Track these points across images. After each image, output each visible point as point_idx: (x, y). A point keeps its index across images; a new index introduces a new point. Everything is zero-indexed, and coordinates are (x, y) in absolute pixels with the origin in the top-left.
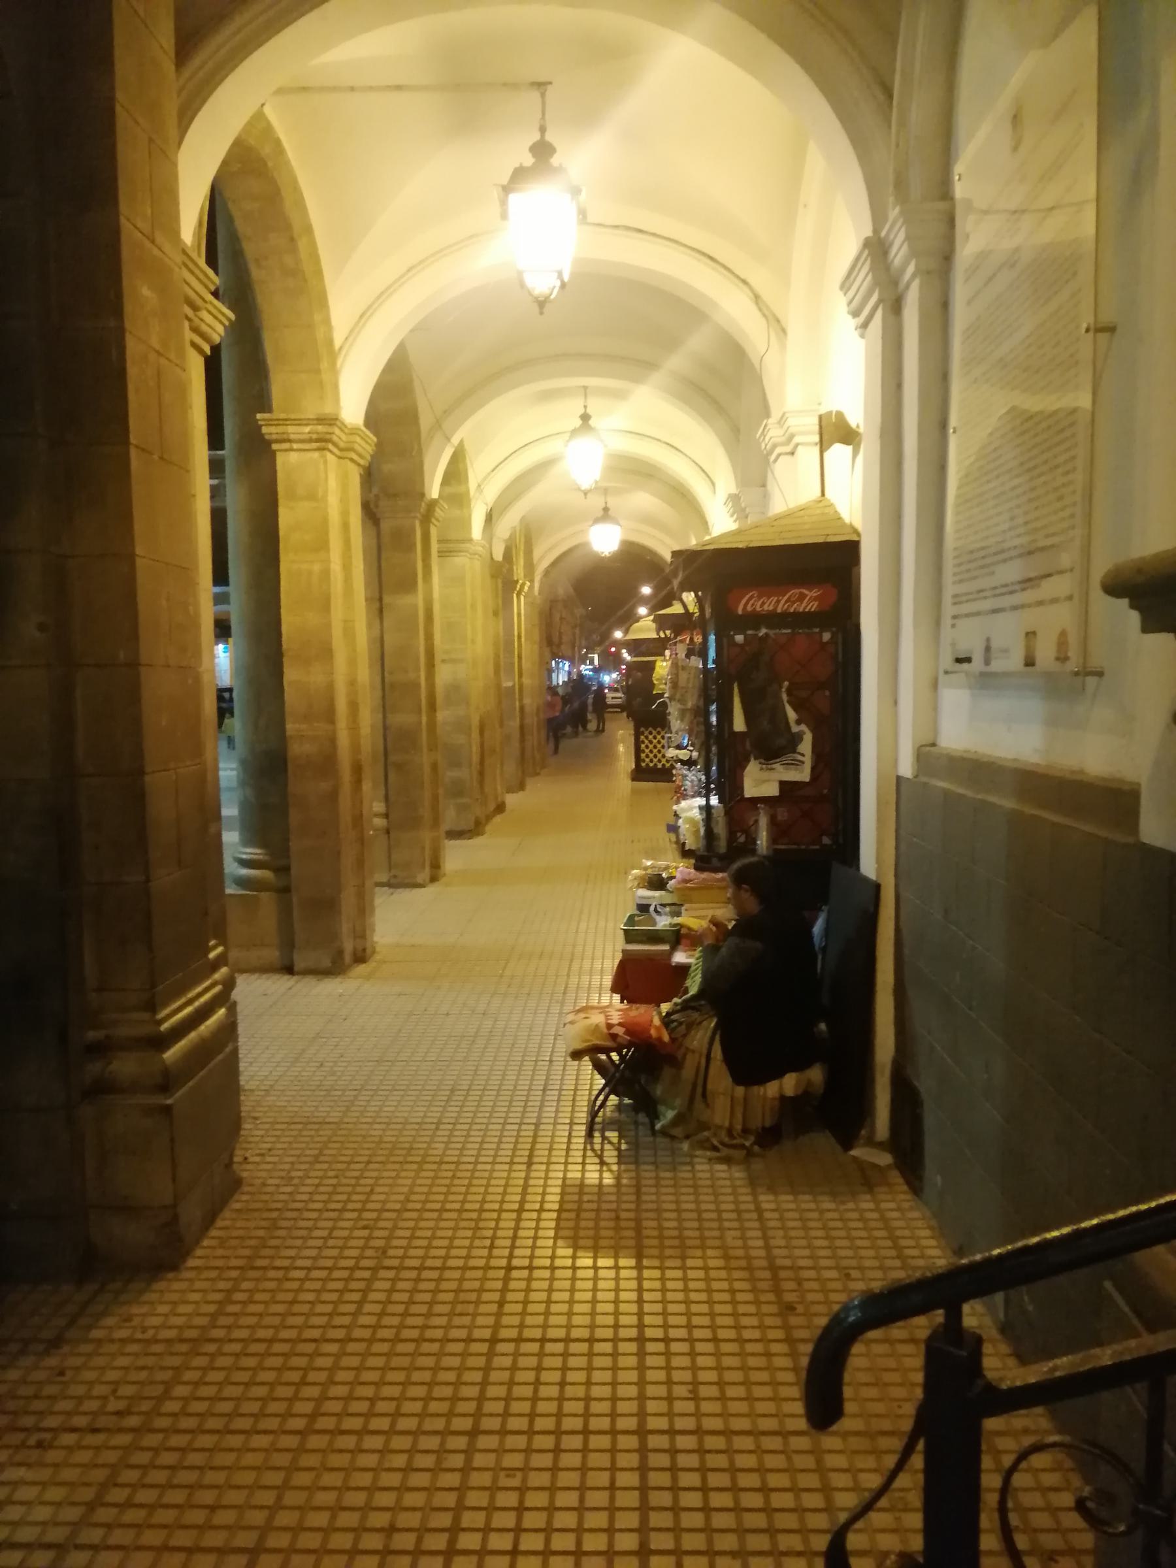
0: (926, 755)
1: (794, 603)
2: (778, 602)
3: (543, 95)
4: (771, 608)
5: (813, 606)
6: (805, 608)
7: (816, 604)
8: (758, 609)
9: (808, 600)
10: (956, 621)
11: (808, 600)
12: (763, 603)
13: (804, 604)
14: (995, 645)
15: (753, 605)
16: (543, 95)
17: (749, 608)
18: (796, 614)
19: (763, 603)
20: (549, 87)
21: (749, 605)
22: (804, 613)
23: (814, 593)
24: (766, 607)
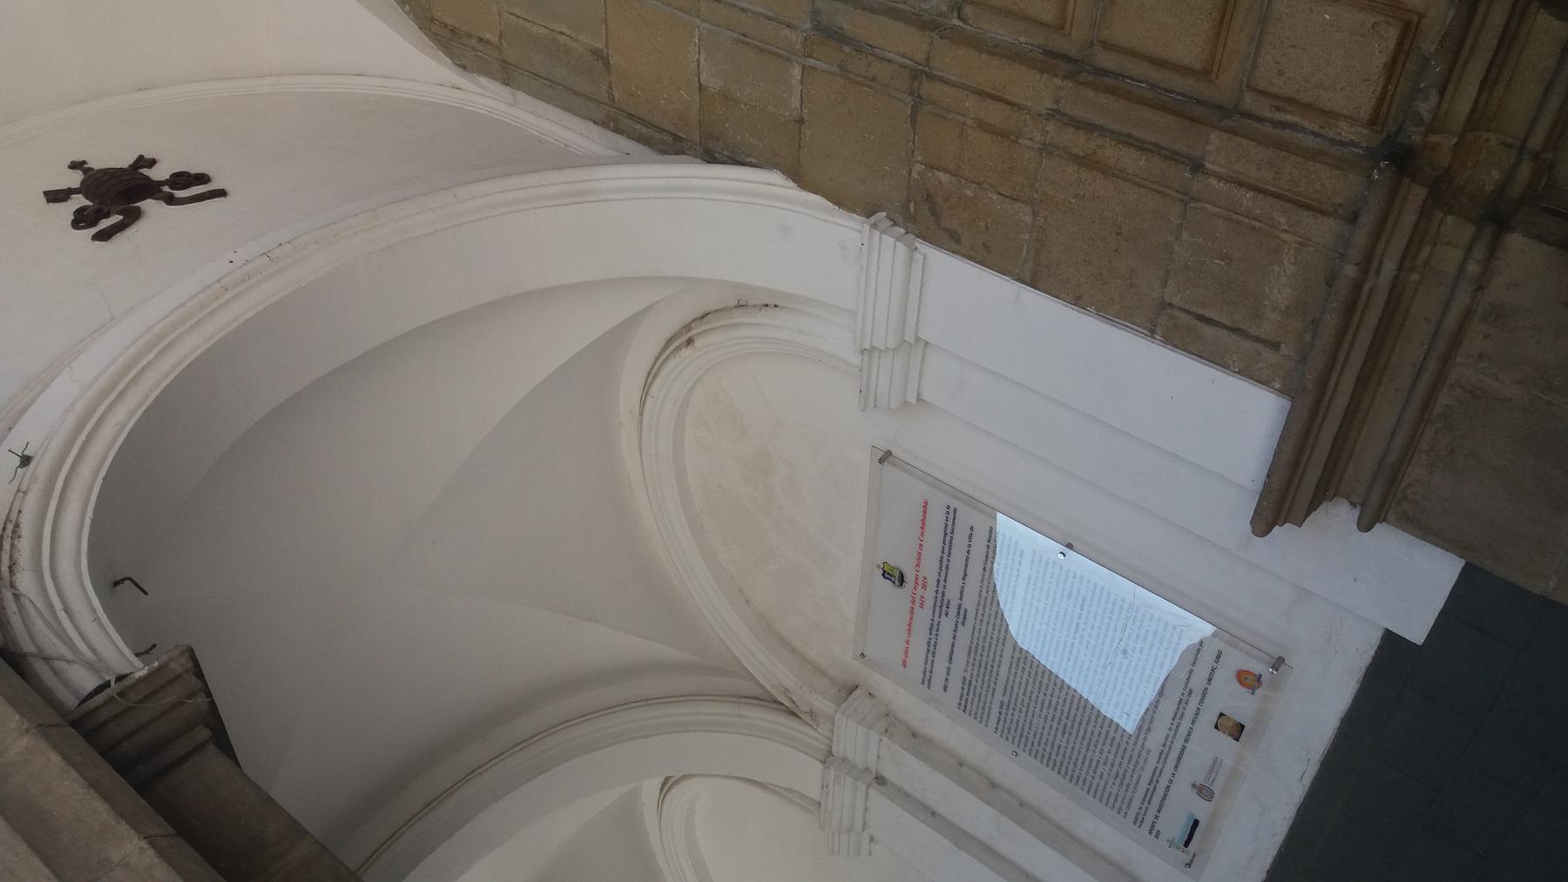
10: (1154, 832)
14: (1200, 781)
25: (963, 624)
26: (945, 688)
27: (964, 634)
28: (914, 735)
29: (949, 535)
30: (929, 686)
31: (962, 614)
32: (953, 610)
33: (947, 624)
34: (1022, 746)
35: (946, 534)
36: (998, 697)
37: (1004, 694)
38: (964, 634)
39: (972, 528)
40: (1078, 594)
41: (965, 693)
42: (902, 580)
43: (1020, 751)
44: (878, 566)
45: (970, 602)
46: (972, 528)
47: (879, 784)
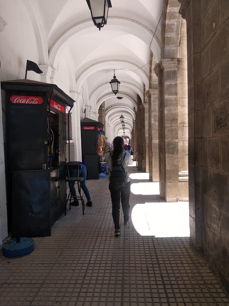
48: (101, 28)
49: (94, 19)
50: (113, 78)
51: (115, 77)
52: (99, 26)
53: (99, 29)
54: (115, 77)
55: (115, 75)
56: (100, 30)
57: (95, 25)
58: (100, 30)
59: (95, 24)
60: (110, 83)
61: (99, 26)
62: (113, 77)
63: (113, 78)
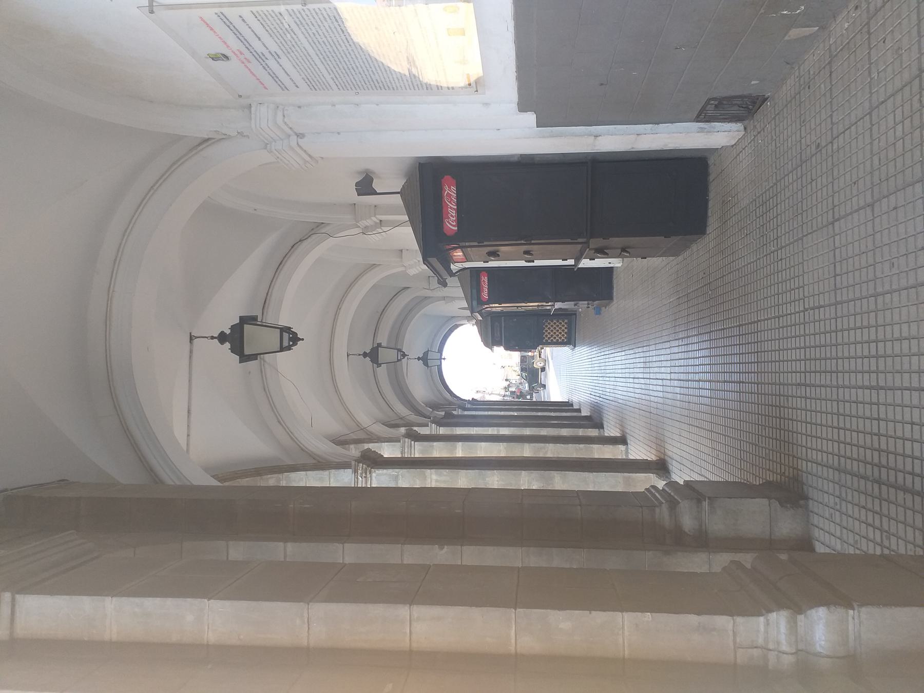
0: (523, 107)
1: (452, 200)
2: (451, 208)
3: (197, 337)
4: (454, 212)
5: (453, 188)
6: (454, 193)
7: (452, 187)
8: (454, 219)
9: (450, 192)
11: (450, 192)
12: (452, 216)
13: (453, 194)
15: (452, 221)
16: (197, 337)
17: (454, 224)
18: (457, 198)
19: (452, 216)
20: (192, 334)
21: (452, 223)
22: (457, 194)
23: (446, 188)
24: (454, 215)
25: (279, 57)
26: (297, 86)
27: (284, 61)
28: (299, 107)
29: (231, 26)
30: (288, 90)
31: (276, 56)
32: (268, 55)
33: (272, 63)
34: (358, 89)
35: (228, 26)
36: (328, 77)
37: (330, 74)
38: (284, 61)
39: (240, 16)
40: (329, 16)
41: (309, 83)
42: (227, 58)
43: (359, 91)
44: (206, 58)
45: (274, 47)
46: (240, 16)
47: (301, 138)
48: (298, 336)
49: (282, 349)
50: (368, 359)
51: (365, 355)
52: (295, 339)
53: (301, 341)
54: (365, 355)
55: (359, 355)
56: (303, 339)
57: (292, 350)
58: (303, 339)
59: (289, 348)
60: (379, 365)
61: (295, 339)
62: (365, 358)
63: (368, 359)
